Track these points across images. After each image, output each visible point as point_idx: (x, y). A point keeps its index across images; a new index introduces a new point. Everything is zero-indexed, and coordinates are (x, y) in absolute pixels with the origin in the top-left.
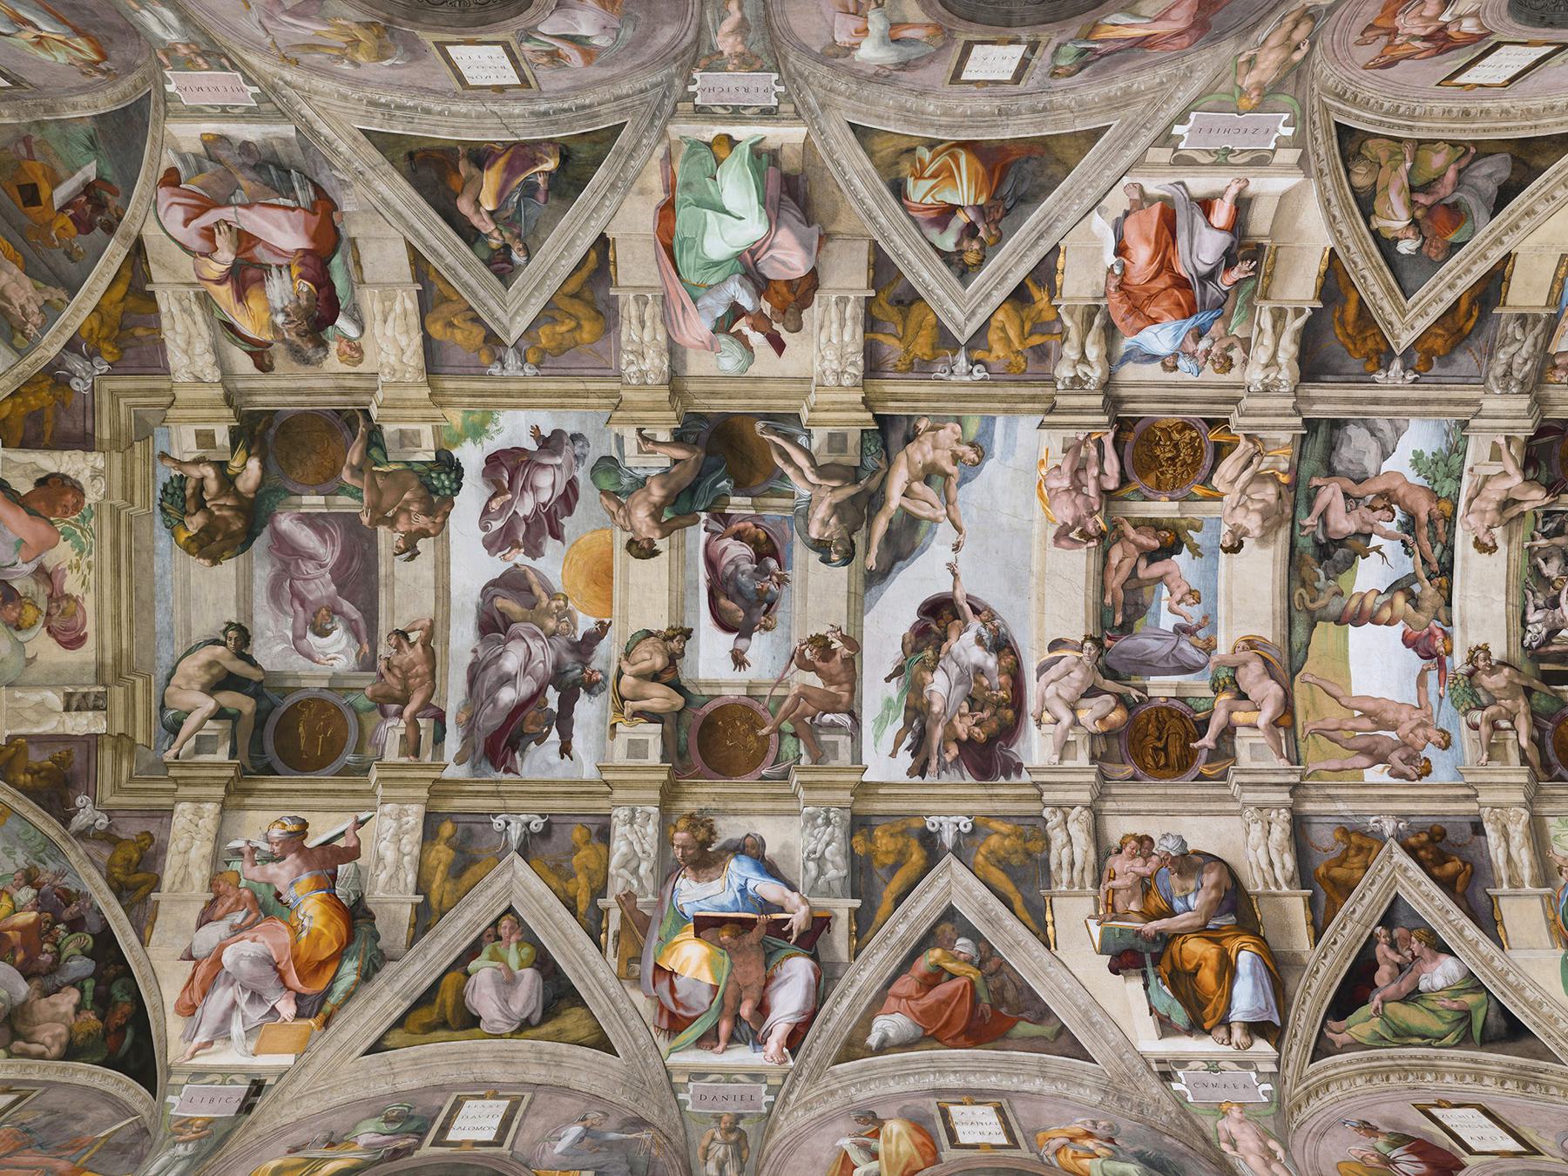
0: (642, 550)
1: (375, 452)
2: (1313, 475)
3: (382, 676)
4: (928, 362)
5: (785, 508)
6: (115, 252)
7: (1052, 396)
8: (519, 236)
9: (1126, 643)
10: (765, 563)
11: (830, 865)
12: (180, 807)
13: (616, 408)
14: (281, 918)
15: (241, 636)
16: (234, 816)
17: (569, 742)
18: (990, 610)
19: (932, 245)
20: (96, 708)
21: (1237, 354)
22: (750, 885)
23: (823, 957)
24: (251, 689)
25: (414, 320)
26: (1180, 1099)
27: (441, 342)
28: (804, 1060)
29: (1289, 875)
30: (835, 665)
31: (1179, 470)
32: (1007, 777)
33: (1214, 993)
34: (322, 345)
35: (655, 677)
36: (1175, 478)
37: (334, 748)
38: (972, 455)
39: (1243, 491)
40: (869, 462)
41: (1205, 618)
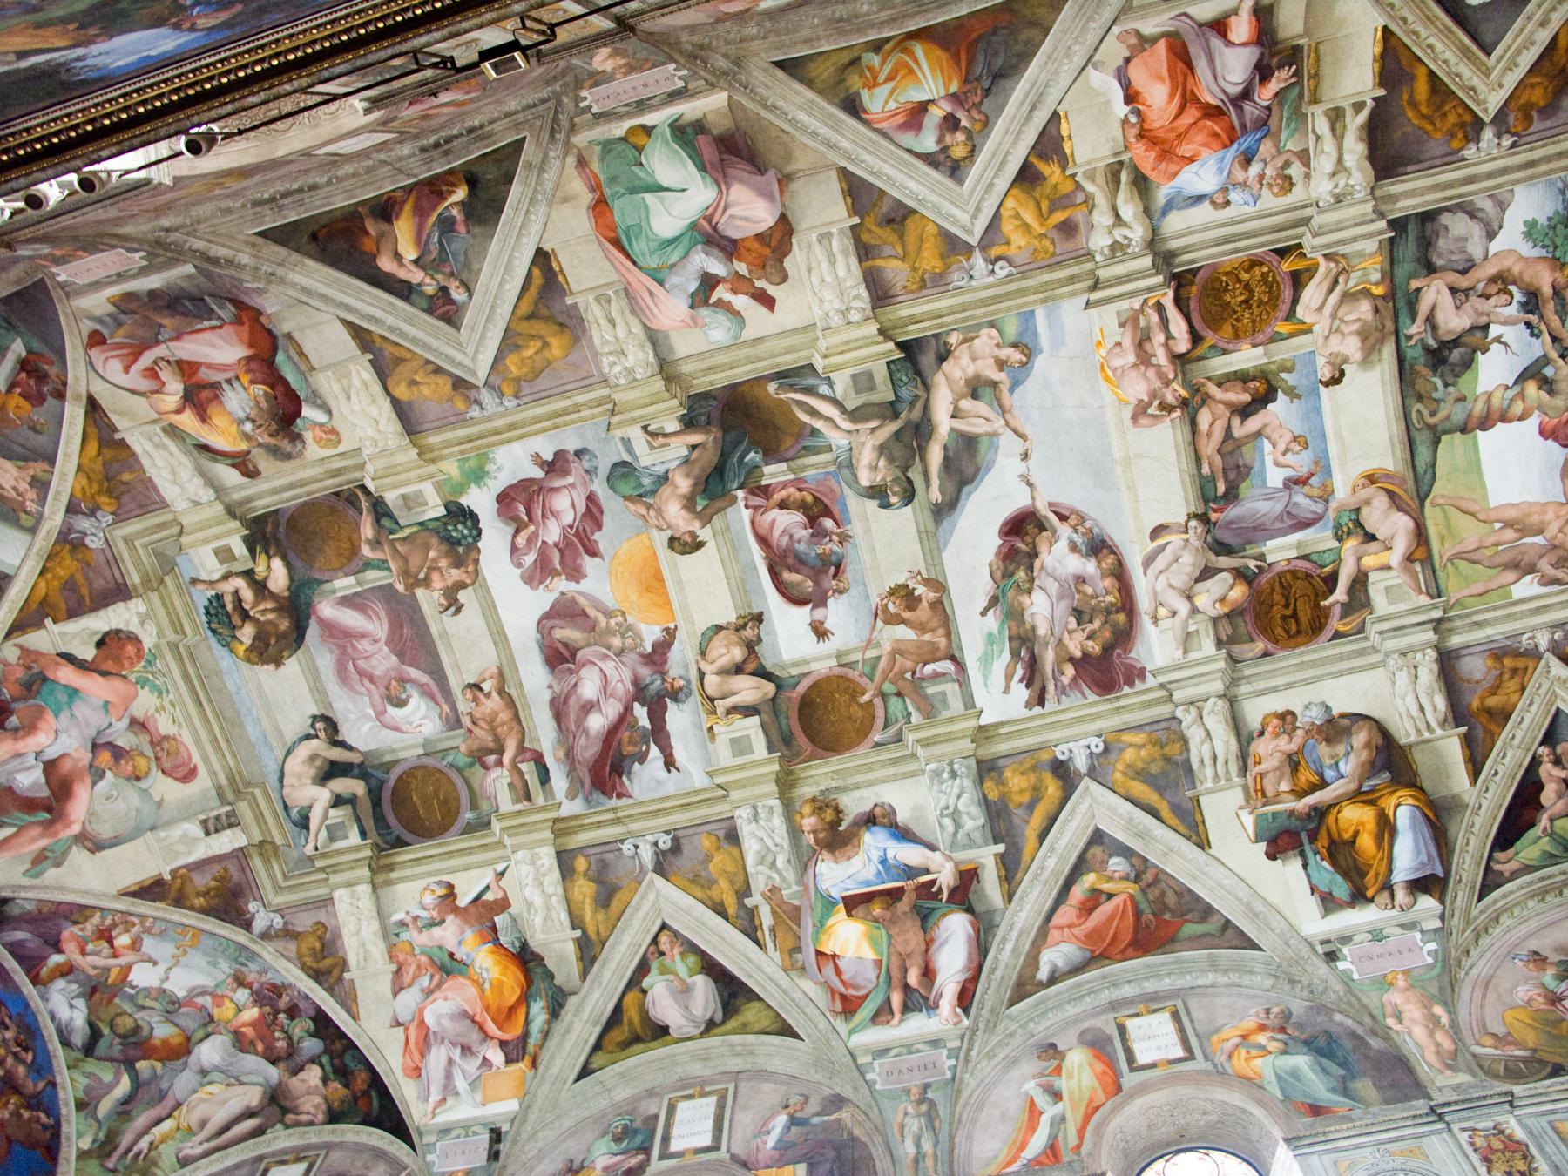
0: (686, 545)
1: (386, 522)
2: (1411, 277)
3: (470, 731)
4: (941, 275)
5: (827, 464)
6: (74, 416)
7: (1092, 272)
8: (452, 274)
9: (1233, 512)
10: (820, 525)
11: (965, 818)
12: (337, 894)
13: (613, 413)
14: (461, 974)
15: (329, 725)
16: (385, 892)
17: (671, 755)
18: (1077, 513)
19: (910, 151)
20: (231, 826)
21: (1296, 171)
22: (890, 855)
23: (978, 908)
24: (356, 771)
25: (377, 388)
26: (1346, 979)
27: (410, 403)
28: (978, 1016)
29: (1441, 716)
30: (923, 612)
31: (1256, 311)
32: (1130, 683)
33: (1374, 858)
34: (296, 438)
35: (738, 669)
36: (1254, 321)
38: (1016, 356)
39: (1334, 316)
40: (905, 393)
41: (1316, 463)
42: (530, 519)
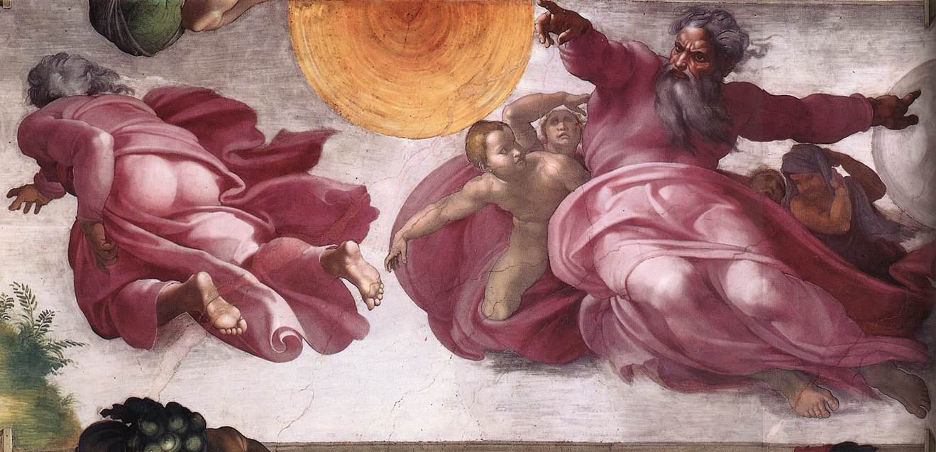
42: (181, 273)
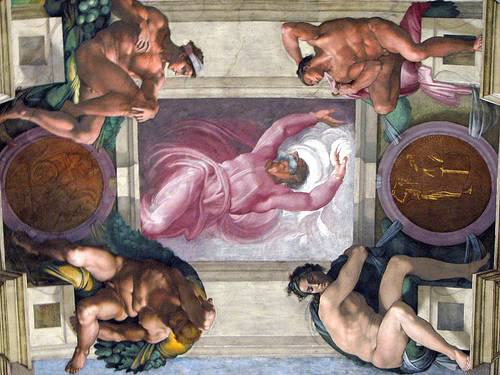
3: (361, 92)
15: (306, 276)
24: (377, 262)
37: (461, 154)
